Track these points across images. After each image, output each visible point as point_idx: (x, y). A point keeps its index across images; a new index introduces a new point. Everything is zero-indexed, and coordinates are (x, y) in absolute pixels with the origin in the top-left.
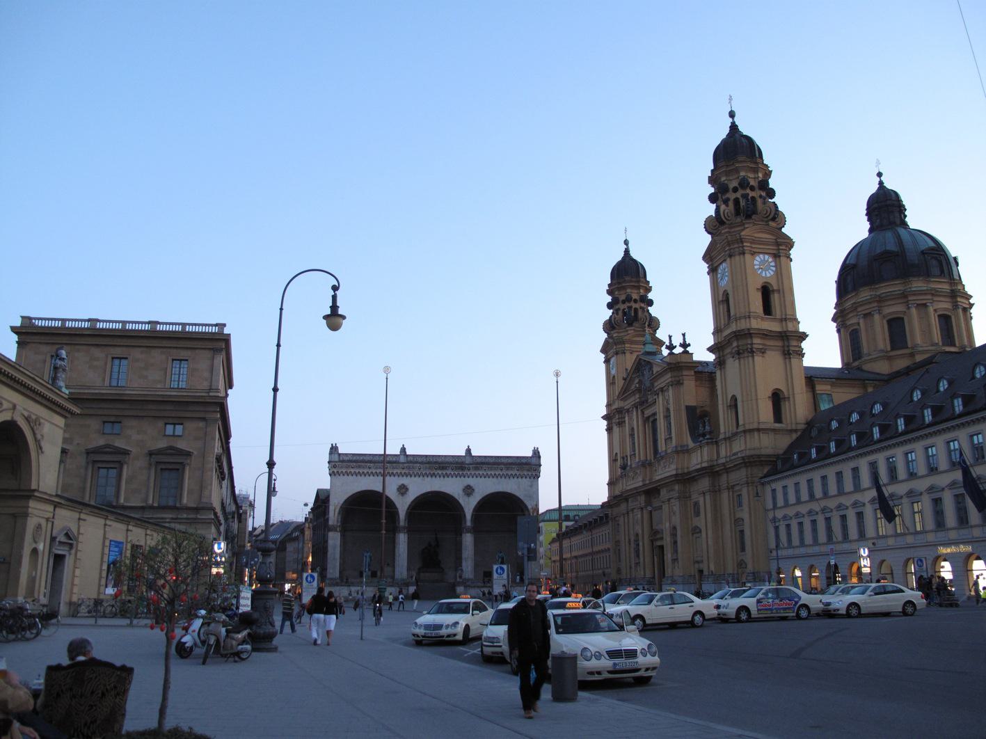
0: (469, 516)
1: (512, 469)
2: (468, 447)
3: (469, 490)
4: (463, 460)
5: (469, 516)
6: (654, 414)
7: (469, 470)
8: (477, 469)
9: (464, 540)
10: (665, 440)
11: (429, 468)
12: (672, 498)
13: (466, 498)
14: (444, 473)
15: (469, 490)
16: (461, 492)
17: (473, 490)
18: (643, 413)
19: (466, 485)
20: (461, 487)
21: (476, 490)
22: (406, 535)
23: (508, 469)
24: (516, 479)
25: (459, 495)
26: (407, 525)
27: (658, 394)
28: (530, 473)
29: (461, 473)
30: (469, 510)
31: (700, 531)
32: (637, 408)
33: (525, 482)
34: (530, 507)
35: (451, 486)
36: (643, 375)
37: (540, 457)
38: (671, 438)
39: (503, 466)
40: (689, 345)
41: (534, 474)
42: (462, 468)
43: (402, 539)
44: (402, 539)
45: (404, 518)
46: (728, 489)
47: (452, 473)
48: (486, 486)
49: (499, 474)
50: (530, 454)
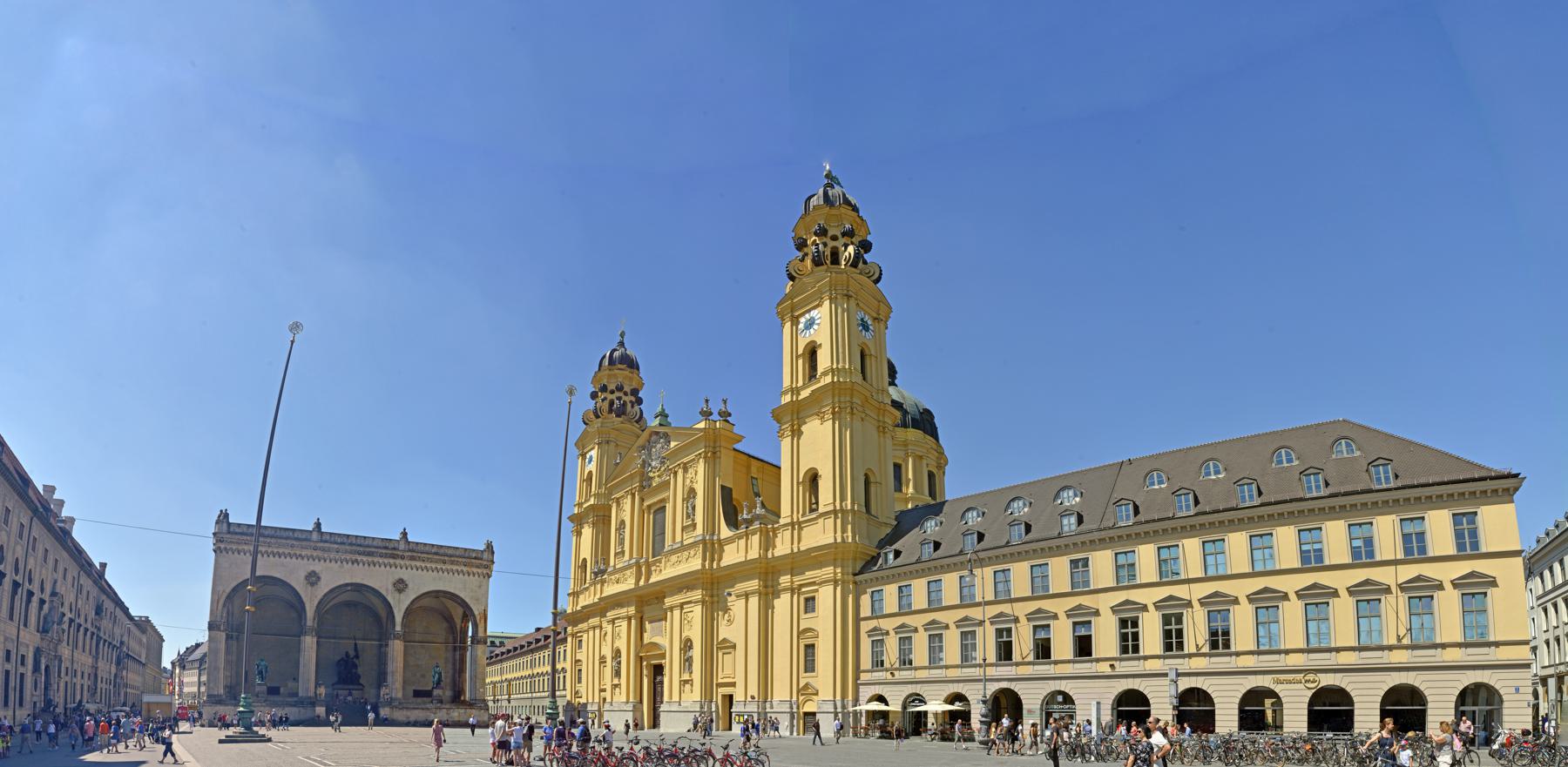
0: (399, 618)
1: (457, 563)
2: (405, 529)
3: (400, 586)
4: (396, 545)
5: (399, 618)
6: (663, 500)
7: (403, 558)
8: (412, 558)
9: (389, 650)
10: (683, 529)
11: (351, 553)
12: (690, 602)
13: (397, 595)
14: (370, 560)
15: (400, 586)
16: (390, 587)
17: (406, 585)
18: (642, 500)
19: (397, 577)
20: (392, 580)
21: (410, 586)
22: (315, 640)
23: (452, 563)
24: (461, 575)
25: (387, 590)
26: (316, 625)
27: (676, 473)
28: (480, 571)
29: (392, 561)
30: (400, 610)
31: (734, 647)
32: (633, 495)
33: (474, 580)
34: (476, 613)
35: (379, 578)
36: (650, 454)
37: (493, 553)
38: (694, 526)
39: (446, 558)
40: (730, 415)
41: (485, 572)
42: (394, 557)
43: (309, 642)
44: (309, 642)
45: (312, 618)
46: (792, 591)
47: (381, 561)
48: (423, 581)
49: (442, 569)
50: (482, 547)
